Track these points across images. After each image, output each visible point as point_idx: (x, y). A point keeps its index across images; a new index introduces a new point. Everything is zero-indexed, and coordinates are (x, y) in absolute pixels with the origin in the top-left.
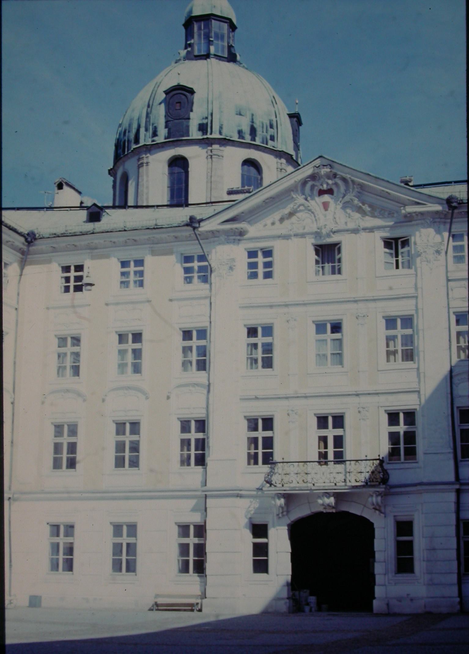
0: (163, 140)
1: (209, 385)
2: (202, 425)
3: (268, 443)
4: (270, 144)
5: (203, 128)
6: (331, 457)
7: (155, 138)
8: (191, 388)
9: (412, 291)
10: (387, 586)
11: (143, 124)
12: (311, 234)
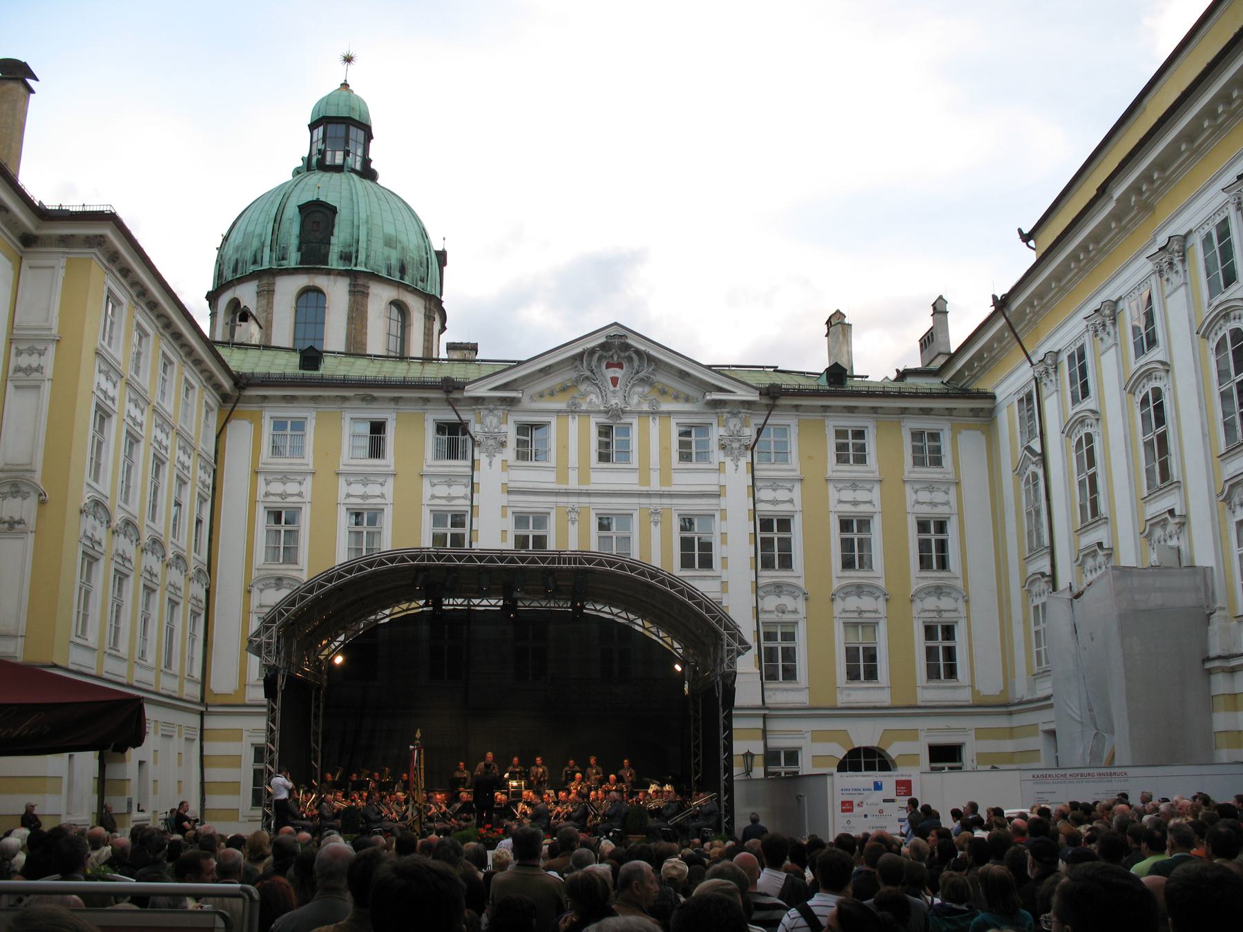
0: (293, 265)
4: (420, 286)
5: (346, 257)
11: (268, 243)
12: (600, 412)
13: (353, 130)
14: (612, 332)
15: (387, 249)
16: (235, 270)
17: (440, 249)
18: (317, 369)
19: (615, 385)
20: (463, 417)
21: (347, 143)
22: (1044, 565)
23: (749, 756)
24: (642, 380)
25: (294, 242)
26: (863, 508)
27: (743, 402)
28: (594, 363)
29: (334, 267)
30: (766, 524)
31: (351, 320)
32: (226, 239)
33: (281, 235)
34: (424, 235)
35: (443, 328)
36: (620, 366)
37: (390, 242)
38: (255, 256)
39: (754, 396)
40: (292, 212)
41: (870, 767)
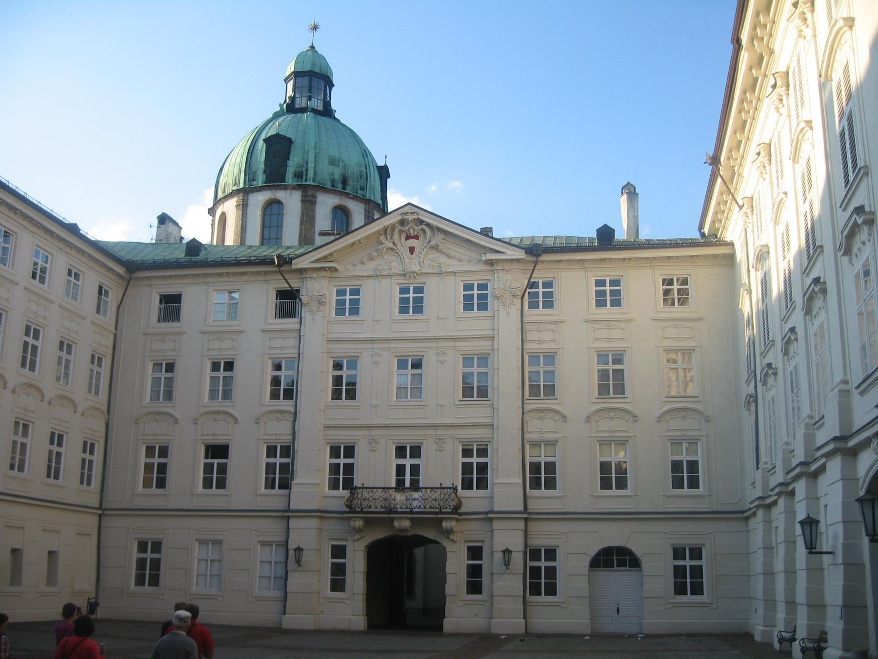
2: (287, 451)
3: (349, 469)
5: (299, 175)
6: (407, 484)
7: (254, 183)
8: (279, 416)
9: (489, 333)
10: (461, 613)
13: (315, 80)
15: (331, 167)
19: (412, 254)
20: (293, 285)
23: (507, 552)
24: (432, 248)
25: (262, 166)
26: (615, 345)
27: (512, 260)
29: (290, 183)
30: (535, 358)
31: (302, 222)
32: (221, 169)
33: (252, 163)
34: (365, 153)
36: (416, 237)
37: (333, 162)
39: (521, 255)
40: (261, 145)
41: (621, 564)
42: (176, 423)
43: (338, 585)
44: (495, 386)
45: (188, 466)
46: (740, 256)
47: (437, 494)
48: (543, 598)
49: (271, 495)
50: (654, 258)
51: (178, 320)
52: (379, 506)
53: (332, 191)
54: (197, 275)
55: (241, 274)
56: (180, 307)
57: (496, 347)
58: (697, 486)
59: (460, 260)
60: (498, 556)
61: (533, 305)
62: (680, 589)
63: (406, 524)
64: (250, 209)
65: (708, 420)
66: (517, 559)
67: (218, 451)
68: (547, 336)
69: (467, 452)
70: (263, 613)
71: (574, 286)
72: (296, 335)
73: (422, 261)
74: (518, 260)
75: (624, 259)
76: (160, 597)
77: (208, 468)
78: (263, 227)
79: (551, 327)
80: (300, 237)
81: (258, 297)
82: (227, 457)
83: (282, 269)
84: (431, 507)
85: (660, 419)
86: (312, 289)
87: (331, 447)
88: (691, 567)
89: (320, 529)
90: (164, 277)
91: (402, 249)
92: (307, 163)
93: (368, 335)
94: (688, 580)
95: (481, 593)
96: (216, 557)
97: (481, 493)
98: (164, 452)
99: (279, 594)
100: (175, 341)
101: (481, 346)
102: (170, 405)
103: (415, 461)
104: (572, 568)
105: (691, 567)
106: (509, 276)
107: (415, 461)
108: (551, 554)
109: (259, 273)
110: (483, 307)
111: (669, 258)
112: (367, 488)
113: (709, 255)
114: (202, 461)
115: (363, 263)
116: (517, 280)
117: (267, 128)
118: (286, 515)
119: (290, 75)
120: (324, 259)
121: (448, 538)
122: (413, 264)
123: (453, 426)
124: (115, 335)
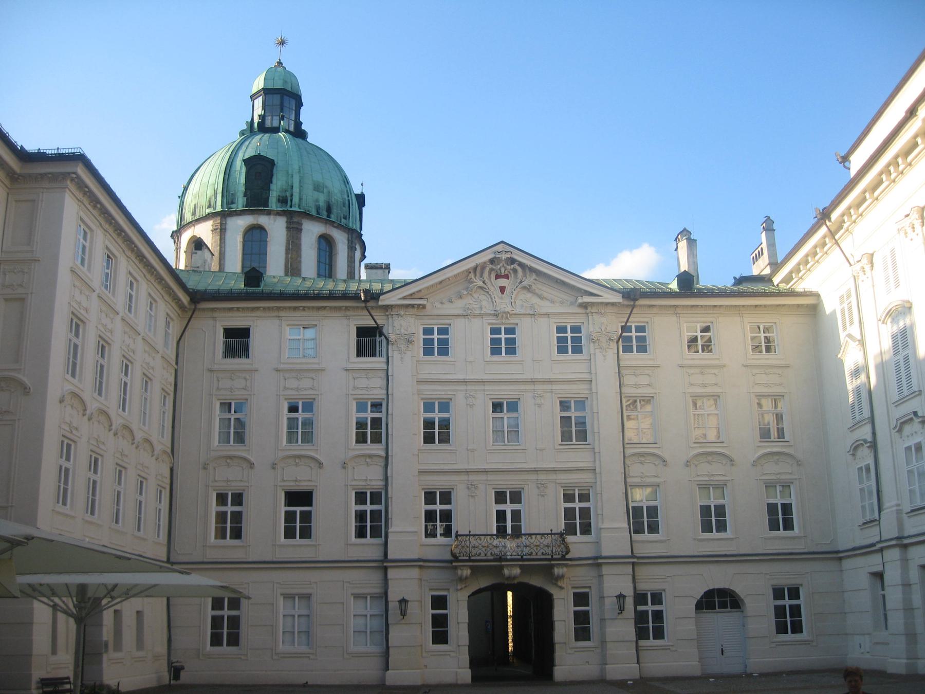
1: (387, 458)
3: (447, 516)
5: (283, 200)
6: (509, 531)
8: (368, 460)
9: (586, 376)
10: (571, 660)
13: (286, 98)
14: (500, 248)
15: (316, 193)
16: (194, 214)
17: (359, 193)
18: (259, 286)
19: (503, 293)
20: (379, 322)
21: (282, 110)
22: (865, 432)
23: (621, 597)
24: (524, 288)
27: (607, 304)
28: (486, 275)
29: (274, 208)
33: (230, 184)
34: (346, 181)
35: (364, 257)
36: (507, 277)
37: (318, 188)
38: (210, 202)
39: (618, 298)
41: (723, 605)
42: (320, 468)
43: (440, 637)
44: (596, 430)
45: (265, 514)
46: (830, 305)
47: (548, 540)
48: (652, 642)
49: (363, 545)
50: (743, 306)
51: (247, 357)
52: (489, 554)
53: (316, 218)
54: (269, 309)
55: (319, 308)
56: (248, 342)
57: (594, 391)
58: (725, 530)
59: (553, 302)
60: (610, 603)
61: (628, 349)
62: (781, 629)
63: (517, 571)
64: (229, 234)
65: (799, 463)
66: (629, 603)
67: (300, 498)
68: (644, 380)
69: (568, 498)
70: (365, 670)
71: (668, 332)
72: (383, 375)
73: (514, 301)
74: (613, 304)
75: (715, 306)
76: (243, 657)
77: (290, 517)
78: (243, 254)
79: (647, 371)
80: (286, 266)
81: (337, 334)
82: (311, 505)
83: (369, 304)
84: (543, 554)
85: (754, 464)
86: (399, 327)
87: (496, 492)
88: (790, 606)
89: (421, 579)
90: (231, 309)
91: (492, 288)
92: (292, 187)
93: (461, 377)
94: (788, 619)
95: (801, 632)
96: (305, 612)
97: (585, 538)
98: (238, 499)
99: (376, 649)
100: (245, 378)
101: (579, 390)
102: (244, 448)
103: (516, 507)
104: (679, 610)
105: (790, 606)
106: (604, 320)
107: (516, 507)
108: (657, 598)
109: (340, 308)
110: (577, 350)
111: (756, 306)
112: (474, 535)
113: (794, 305)
114: (283, 509)
115: (451, 302)
116: (612, 324)
117: (244, 148)
118: (384, 564)
119: (259, 92)
120: (411, 296)
121: (556, 585)
122: (503, 304)
123: (555, 471)
124: (176, 371)
